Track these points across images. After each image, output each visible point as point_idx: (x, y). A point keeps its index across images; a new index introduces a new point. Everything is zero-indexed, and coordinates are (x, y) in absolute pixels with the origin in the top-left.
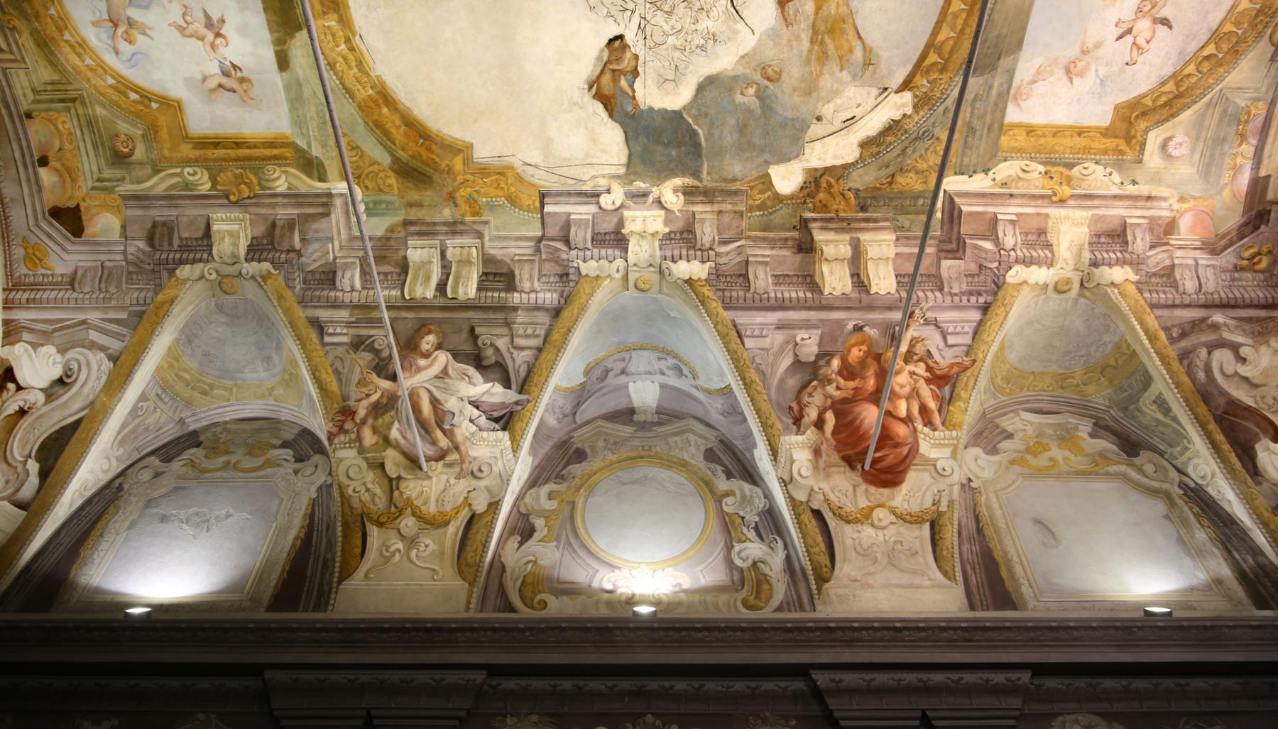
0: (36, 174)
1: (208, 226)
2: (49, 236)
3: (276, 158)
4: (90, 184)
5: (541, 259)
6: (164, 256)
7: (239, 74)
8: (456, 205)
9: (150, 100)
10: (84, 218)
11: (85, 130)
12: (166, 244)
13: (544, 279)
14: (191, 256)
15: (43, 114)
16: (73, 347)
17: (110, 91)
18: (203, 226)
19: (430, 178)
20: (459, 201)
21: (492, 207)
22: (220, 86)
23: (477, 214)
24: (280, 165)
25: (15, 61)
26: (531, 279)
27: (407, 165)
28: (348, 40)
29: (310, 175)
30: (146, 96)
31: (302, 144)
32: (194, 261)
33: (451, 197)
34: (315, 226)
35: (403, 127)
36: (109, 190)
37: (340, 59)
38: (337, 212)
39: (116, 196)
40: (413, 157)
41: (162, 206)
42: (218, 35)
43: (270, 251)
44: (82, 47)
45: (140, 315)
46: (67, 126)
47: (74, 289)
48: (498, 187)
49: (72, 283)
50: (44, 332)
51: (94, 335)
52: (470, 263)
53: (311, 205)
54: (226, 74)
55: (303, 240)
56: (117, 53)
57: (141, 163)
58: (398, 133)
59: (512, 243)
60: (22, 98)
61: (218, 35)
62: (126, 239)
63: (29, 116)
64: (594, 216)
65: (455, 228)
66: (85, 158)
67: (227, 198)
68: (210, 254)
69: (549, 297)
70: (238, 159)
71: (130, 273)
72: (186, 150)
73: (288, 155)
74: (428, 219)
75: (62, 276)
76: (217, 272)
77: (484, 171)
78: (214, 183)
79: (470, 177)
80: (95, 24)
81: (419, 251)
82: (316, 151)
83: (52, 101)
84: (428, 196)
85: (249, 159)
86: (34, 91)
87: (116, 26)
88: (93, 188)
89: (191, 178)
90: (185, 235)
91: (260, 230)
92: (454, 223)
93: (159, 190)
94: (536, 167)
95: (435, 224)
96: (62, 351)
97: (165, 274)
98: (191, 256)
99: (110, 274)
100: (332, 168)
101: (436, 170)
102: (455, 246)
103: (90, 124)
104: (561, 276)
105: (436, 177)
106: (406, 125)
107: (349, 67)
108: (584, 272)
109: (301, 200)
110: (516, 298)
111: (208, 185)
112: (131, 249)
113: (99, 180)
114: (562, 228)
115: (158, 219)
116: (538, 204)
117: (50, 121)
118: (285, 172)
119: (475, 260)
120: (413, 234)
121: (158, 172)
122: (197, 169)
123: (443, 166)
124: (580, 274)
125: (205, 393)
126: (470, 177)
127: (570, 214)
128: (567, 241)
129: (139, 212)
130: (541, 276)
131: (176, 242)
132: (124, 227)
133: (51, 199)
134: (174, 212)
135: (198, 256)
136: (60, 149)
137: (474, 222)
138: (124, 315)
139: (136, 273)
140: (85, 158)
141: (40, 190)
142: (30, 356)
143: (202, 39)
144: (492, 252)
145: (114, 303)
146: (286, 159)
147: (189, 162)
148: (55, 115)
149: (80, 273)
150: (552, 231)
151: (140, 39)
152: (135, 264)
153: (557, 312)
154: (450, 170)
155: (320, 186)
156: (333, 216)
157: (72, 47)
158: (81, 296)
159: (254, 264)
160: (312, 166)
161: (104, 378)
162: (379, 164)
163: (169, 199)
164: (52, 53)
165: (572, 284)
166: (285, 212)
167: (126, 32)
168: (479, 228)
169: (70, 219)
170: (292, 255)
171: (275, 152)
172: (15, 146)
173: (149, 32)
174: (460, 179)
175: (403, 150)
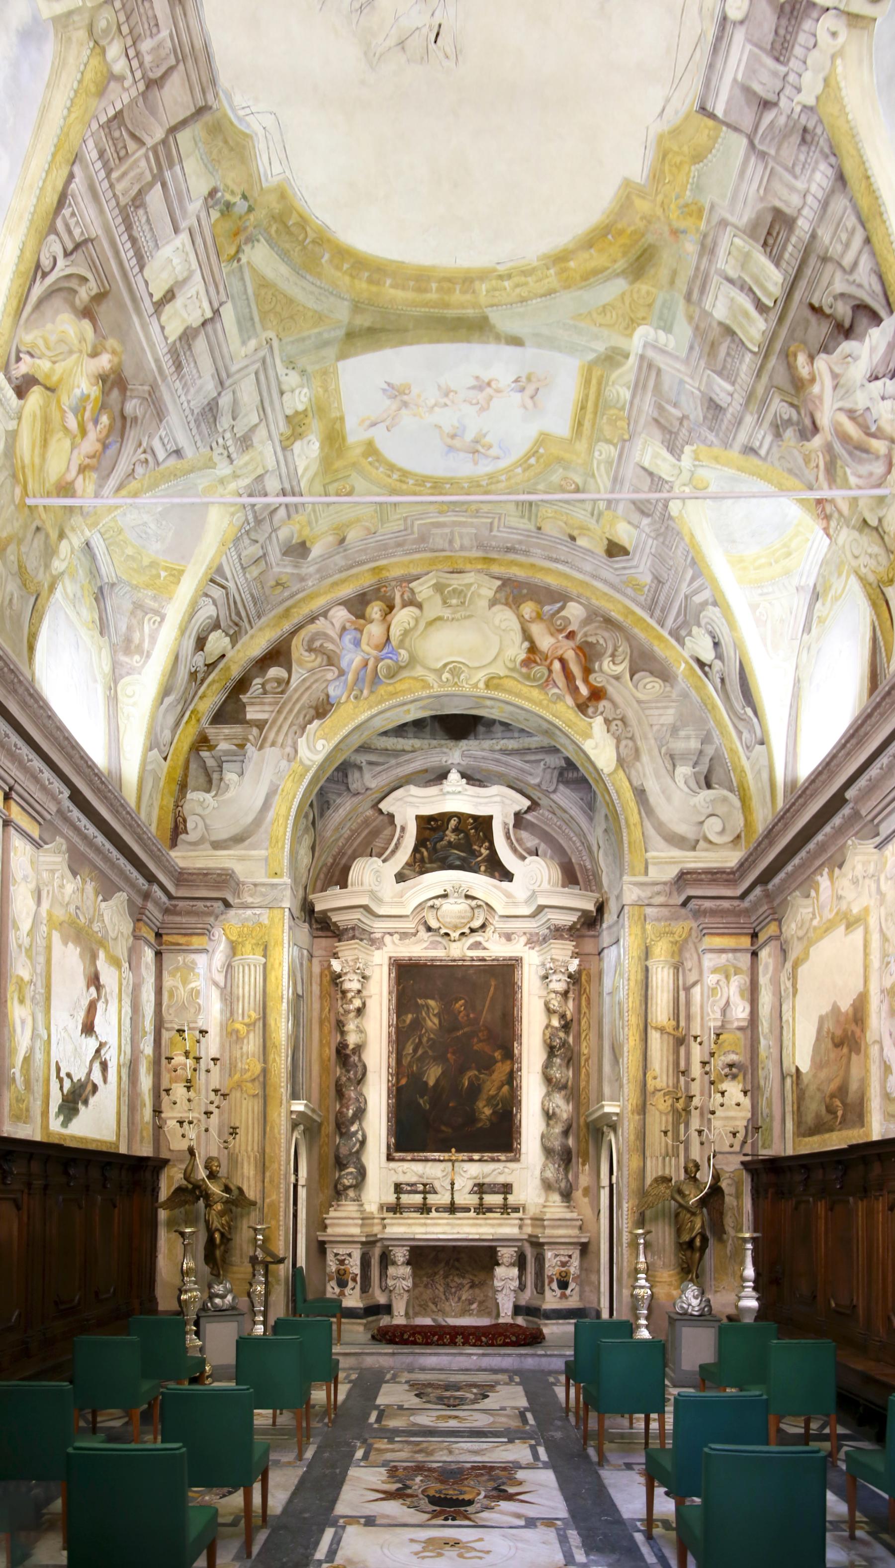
3: (599, 384)
5: (775, 159)
7: (524, 379)
8: (684, 232)
9: (537, 452)
13: (798, 170)
17: (527, 474)
19: (650, 246)
20: (681, 225)
21: (698, 188)
22: (532, 397)
23: (700, 210)
24: (607, 384)
25: (500, 519)
26: (792, 189)
27: (631, 265)
28: (501, 277)
29: (619, 365)
30: (533, 453)
31: (591, 356)
33: (675, 233)
34: (666, 386)
35: (592, 251)
36: (600, 514)
37: (518, 290)
38: (659, 360)
39: (606, 513)
40: (625, 254)
42: (489, 384)
43: (676, 438)
48: (679, 167)
52: (747, 256)
53: (647, 378)
54: (522, 390)
55: (675, 405)
57: (585, 483)
58: (595, 259)
59: (744, 186)
61: (489, 384)
64: (749, 40)
65: (707, 249)
67: (625, 441)
69: (820, 178)
70: (595, 413)
72: (581, 446)
73: (599, 373)
74: (691, 272)
77: (656, 176)
78: (609, 442)
79: (660, 198)
80: (476, 463)
81: (718, 303)
82: (600, 347)
84: (666, 258)
85: (596, 405)
86: (522, 517)
87: (477, 451)
88: (597, 521)
89: (603, 456)
91: (657, 434)
92: (703, 245)
94: (668, 100)
95: (697, 268)
100: (619, 342)
101: (643, 235)
102: (725, 263)
104: (803, 140)
105: (650, 238)
106: (591, 247)
107: (526, 284)
108: (811, 101)
109: (641, 385)
110: (803, 225)
111: (612, 447)
113: (592, 514)
114: (748, 102)
116: (711, 123)
118: (613, 383)
119: (747, 248)
120: (700, 300)
122: (597, 448)
123: (641, 225)
124: (811, 109)
126: (660, 198)
127: (735, 80)
128: (766, 105)
130: (791, 171)
137: (708, 221)
143: (491, 398)
144: (745, 219)
146: (602, 376)
147: (590, 451)
150: (747, 121)
151: (488, 439)
153: (841, 178)
154: (648, 220)
155: (632, 361)
156: (662, 366)
157: (491, 483)
159: (683, 457)
160: (612, 358)
162: (623, 294)
165: (819, 131)
166: (647, 405)
167: (483, 446)
168: (715, 220)
170: (685, 423)
171: (594, 382)
173: (484, 432)
174: (659, 212)
175: (615, 261)
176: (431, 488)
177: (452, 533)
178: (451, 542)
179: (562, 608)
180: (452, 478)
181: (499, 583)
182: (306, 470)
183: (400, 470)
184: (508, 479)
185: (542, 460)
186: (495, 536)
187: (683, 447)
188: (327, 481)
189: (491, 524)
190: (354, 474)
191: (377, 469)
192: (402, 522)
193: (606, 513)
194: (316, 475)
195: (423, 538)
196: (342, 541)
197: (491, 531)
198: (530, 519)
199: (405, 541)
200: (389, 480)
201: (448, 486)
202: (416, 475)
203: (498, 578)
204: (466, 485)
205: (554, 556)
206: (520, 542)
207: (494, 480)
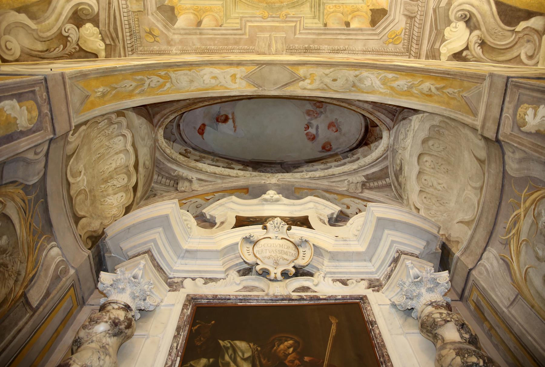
0: (353, 30)
2: (385, 28)
10: (377, 8)
15: (325, 17)
25: (300, 21)
46: (332, 7)
50: (436, 35)
60: (317, 25)
63: (325, 25)
75: (406, 24)
83: (319, 10)
86: (314, 18)
96: (449, 23)
136: (342, 13)
141: (361, 30)
142: (449, 43)
148: (326, 11)
149: (406, 13)
158: (419, 13)
172: (339, 37)
177: (270, 36)
178: (270, 46)
186: (298, 38)
189: (295, 26)
192: (238, 21)
196: (199, 23)
197: (295, 34)
198: (319, 20)
205: (336, 47)
206: (314, 41)
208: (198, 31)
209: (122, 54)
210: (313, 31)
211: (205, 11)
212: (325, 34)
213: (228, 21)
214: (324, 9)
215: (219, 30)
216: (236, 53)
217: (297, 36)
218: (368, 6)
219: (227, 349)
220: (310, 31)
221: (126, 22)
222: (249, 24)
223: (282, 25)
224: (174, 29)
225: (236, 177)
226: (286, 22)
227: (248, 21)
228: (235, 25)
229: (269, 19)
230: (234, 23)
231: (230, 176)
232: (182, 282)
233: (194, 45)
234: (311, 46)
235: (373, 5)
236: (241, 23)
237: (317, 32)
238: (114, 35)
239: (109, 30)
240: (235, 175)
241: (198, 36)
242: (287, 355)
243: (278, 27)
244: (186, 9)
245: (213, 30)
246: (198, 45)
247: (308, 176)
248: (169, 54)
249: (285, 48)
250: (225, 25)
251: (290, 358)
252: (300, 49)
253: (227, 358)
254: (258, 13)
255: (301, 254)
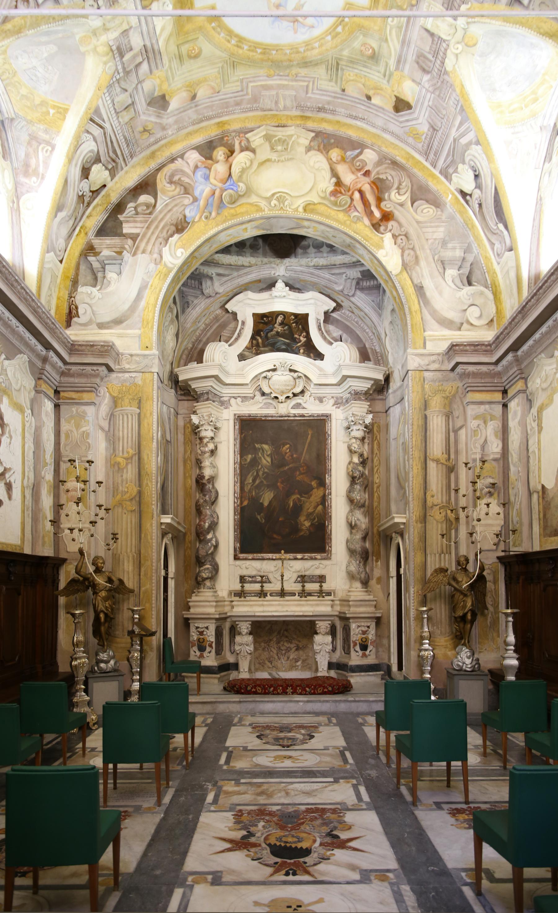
0: (374, 105)
1: (427, 30)
2: (407, 121)
4: (385, 82)
6: (436, 70)
10: (403, 98)
11: (355, 66)
12: (429, 63)
14: (441, 54)
15: (344, 83)
16: (464, 156)
18: (426, 34)
32: (445, 54)
36: (391, 75)
39: (395, 73)
41: (408, 50)
44: (308, 44)
45: (462, 110)
46: (352, 74)
47: (437, 131)
49: (434, 129)
50: (452, 161)
51: (464, 141)
56: (313, 27)
62: (420, 84)
66: (371, 76)
68: (444, 41)
71: (439, 96)
75: (429, 130)
76: (458, 43)
80: (296, 32)
83: (337, 75)
86: (331, 80)
88: (388, 81)
90: (427, 49)
93: (398, 47)
97: (446, 77)
98: (441, 54)
99: (436, 106)
103: (352, 62)
112: (427, 86)
113: (385, 76)
115: (414, 58)
117: (347, 82)
121: (387, 40)
125: (535, 100)
129: (407, 67)
131: (430, 57)
132: (413, 81)
133: (389, 106)
134: (412, 46)
135: (443, 49)
138: (459, 119)
139: (440, 93)
140: (371, 76)
141: (383, 109)
145: (451, 117)
149: (430, 121)
152: (435, 89)
157: (308, 50)
161: (484, 156)
163: (405, 43)
164: (311, 62)
169: (401, 105)
172: (359, 106)
173: (302, 2)
176: (261, 53)
177: (277, 94)
178: (276, 103)
179: (361, 153)
180: (277, 45)
181: (313, 134)
182: (163, 29)
183: (237, 36)
184: (321, 46)
185: (347, 28)
186: (310, 98)
187: (460, 6)
188: (180, 42)
190: (201, 38)
191: (219, 34)
192: (239, 83)
193: (395, 73)
194: (171, 35)
195: (255, 99)
196: (194, 97)
197: (307, 93)
198: (336, 82)
199: (242, 100)
200: (229, 45)
201: (274, 52)
202: (249, 41)
203: (312, 131)
204: (288, 52)
205: (354, 114)
206: (329, 103)
207: (309, 47)
208: (193, 105)
209: (123, 165)
210: (328, 93)
211: (199, 83)
212: (342, 99)
213: (226, 86)
214: (343, 75)
215: (217, 96)
216: (238, 113)
217: (309, 95)
218: (393, 91)
219: (259, 449)
220: (325, 93)
221: (122, 137)
222: (251, 85)
223: (291, 83)
224: (168, 114)
225: (249, 267)
226: (296, 81)
227: (250, 82)
228: (234, 88)
229: (275, 78)
230: (233, 87)
231: (243, 266)
232: (229, 400)
233: (189, 118)
234: (326, 106)
235: (399, 93)
236: (242, 86)
237: (333, 95)
238: (114, 156)
239: (109, 156)
240: (247, 264)
241: (193, 109)
242: (286, 453)
243: (287, 85)
244: (178, 89)
245: (209, 98)
246: (195, 117)
247: (312, 264)
248: (166, 138)
249: (295, 105)
250: (223, 90)
251: (287, 455)
252: (312, 107)
253: (260, 455)
254: (262, 72)
255: (297, 384)
